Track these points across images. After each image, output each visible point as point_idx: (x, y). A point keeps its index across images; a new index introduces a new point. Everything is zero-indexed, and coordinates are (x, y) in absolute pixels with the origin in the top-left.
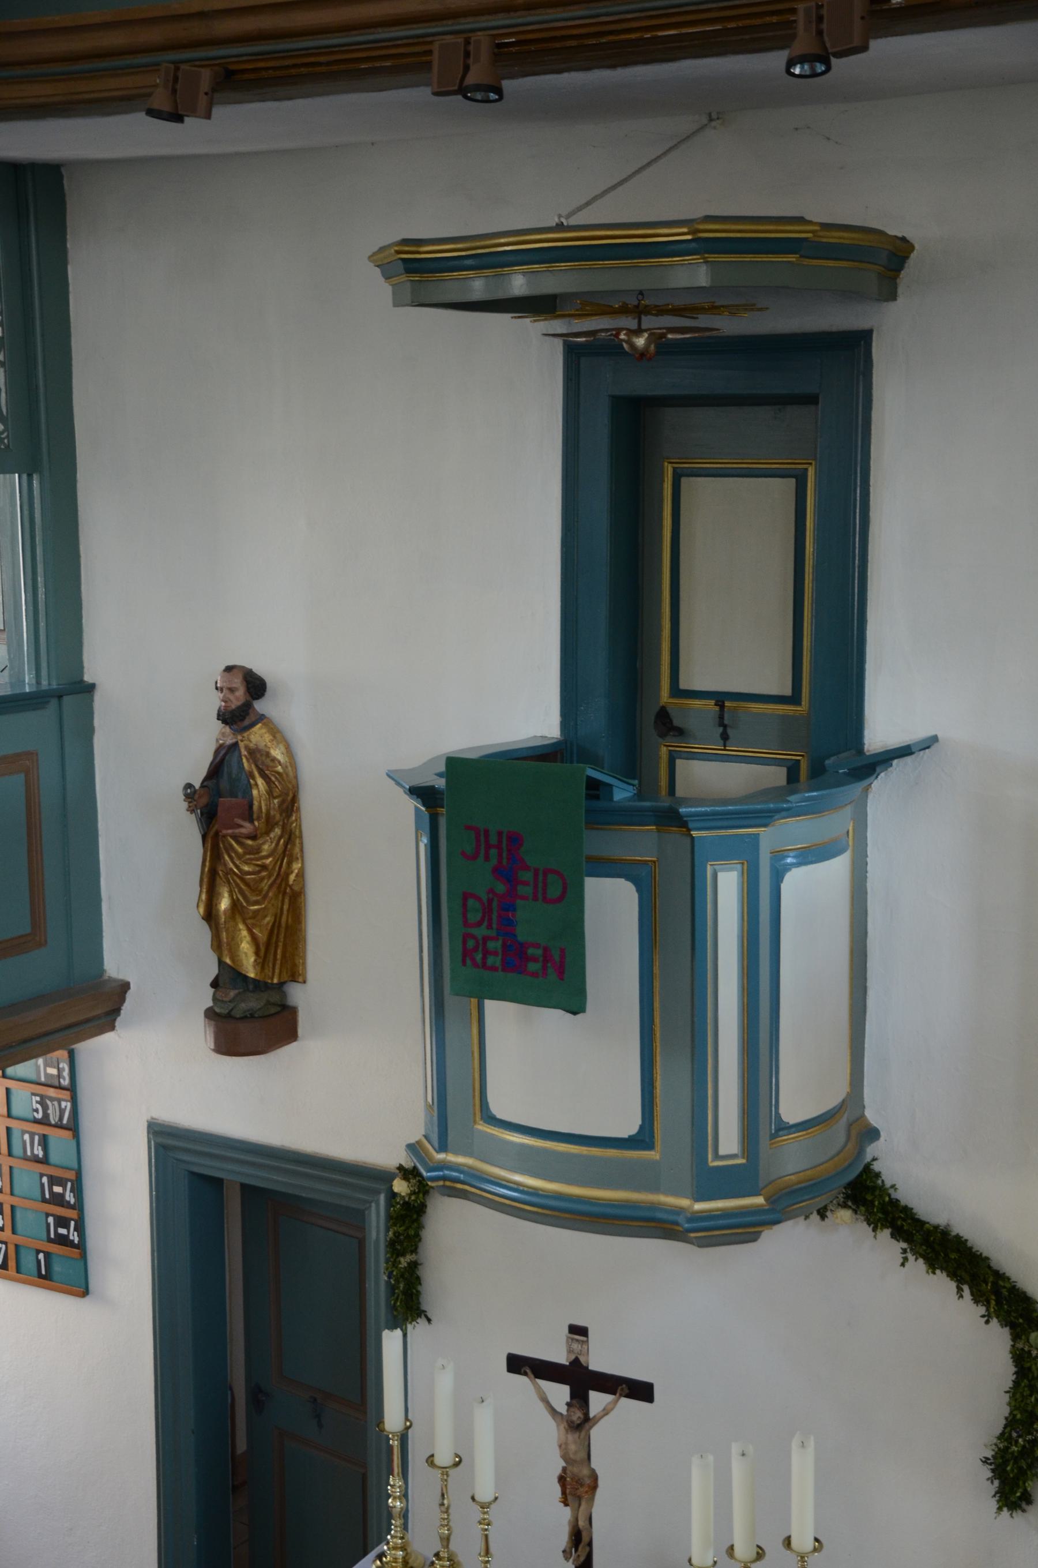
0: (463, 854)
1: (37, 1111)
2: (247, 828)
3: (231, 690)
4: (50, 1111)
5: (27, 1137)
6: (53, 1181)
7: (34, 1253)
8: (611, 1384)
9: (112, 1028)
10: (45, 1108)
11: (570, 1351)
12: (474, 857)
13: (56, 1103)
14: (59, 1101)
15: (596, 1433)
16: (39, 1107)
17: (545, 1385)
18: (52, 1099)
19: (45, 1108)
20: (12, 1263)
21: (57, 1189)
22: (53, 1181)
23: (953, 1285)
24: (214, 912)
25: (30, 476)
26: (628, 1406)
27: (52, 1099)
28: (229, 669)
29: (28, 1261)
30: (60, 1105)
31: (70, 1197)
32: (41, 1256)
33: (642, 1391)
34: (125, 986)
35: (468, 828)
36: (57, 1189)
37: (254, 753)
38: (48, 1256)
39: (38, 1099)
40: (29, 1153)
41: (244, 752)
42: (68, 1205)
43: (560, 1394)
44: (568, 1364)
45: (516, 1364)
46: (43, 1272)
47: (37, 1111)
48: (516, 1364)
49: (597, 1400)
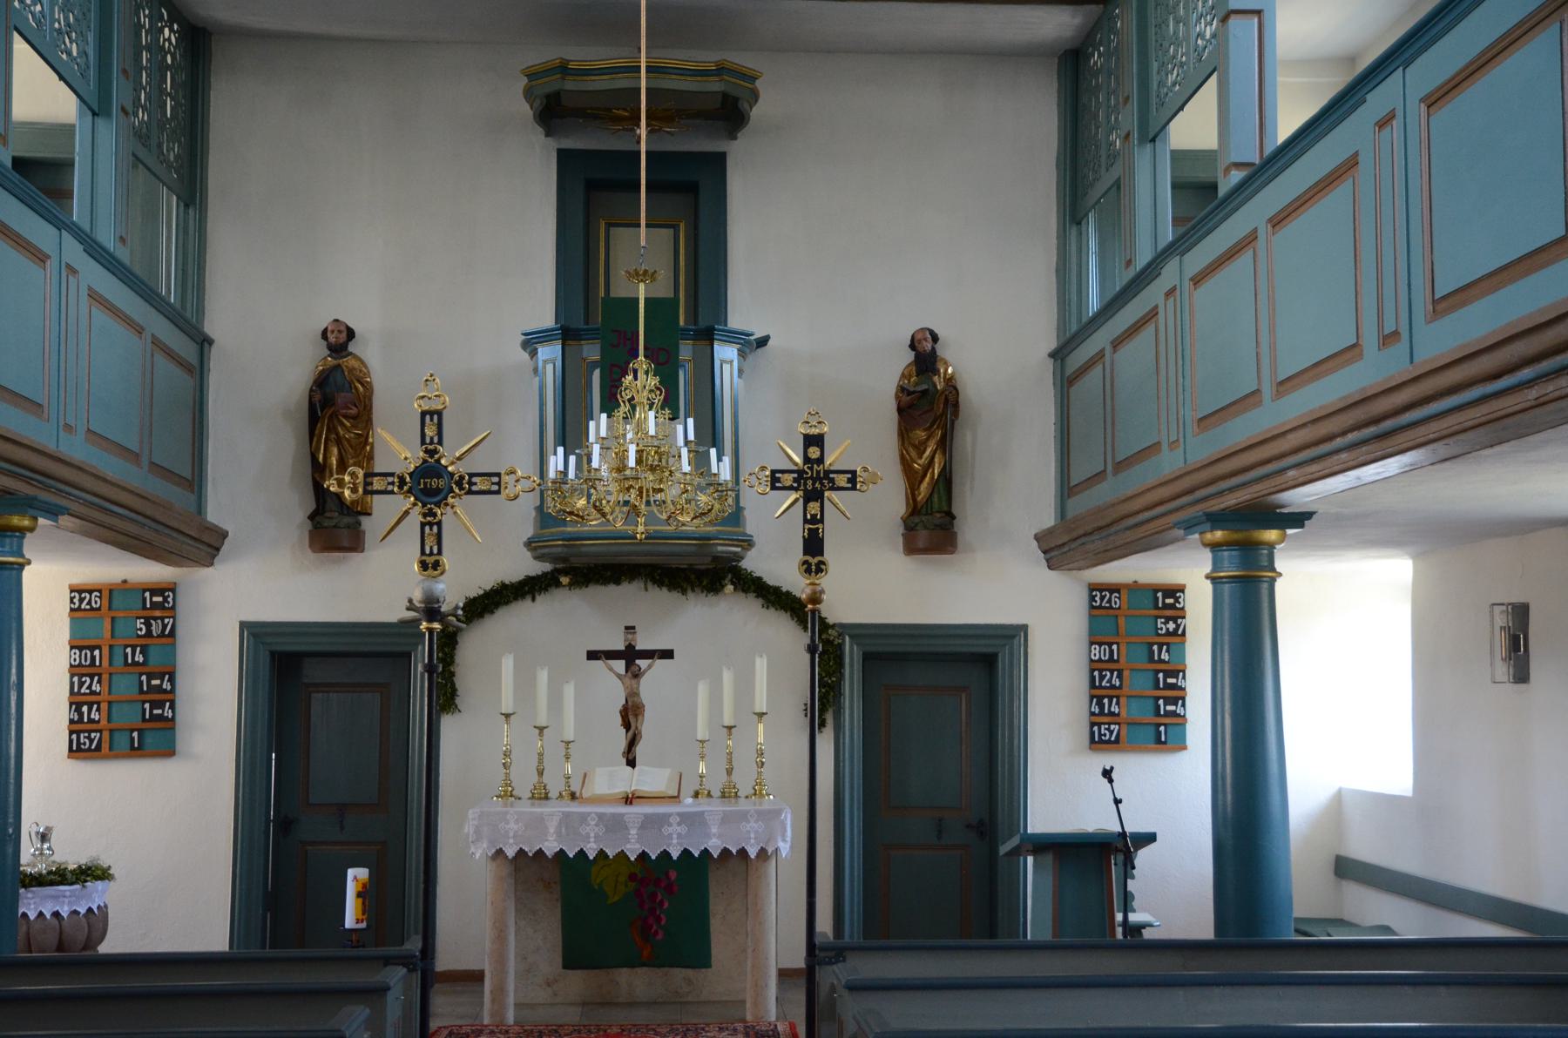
0: (613, 346)
1: (141, 629)
2: (354, 411)
3: (340, 332)
4: (153, 628)
5: (129, 650)
6: (150, 676)
7: (128, 733)
8: (649, 654)
9: (209, 562)
10: (148, 625)
11: (625, 640)
12: (618, 346)
13: (159, 621)
14: (162, 619)
15: (644, 681)
16: (143, 626)
17: (611, 662)
18: (155, 619)
19: (148, 625)
20: (105, 746)
21: (156, 682)
22: (150, 676)
23: (789, 614)
24: (329, 461)
25: (187, 206)
26: (660, 664)
27: (155, 619)
28: (336, 321)
29: (122, 740)
30: (163, 622)
31: (167, 686)
32: (135, 734)
33: (668, 654)
34: (223, 535)
35: (614, 331)
36: (156, 682)
37: (352, 370)
38: (140, 731)
39: (142, 621)
40: (130, 661)
41: (345, 368)
42: (165, 691)
43: (620, 665)
44: (624, 648)
45: (593, 655)
46: (136, 745)
47: (141, 629)
48: (593, 655)
49: (643, 663)
